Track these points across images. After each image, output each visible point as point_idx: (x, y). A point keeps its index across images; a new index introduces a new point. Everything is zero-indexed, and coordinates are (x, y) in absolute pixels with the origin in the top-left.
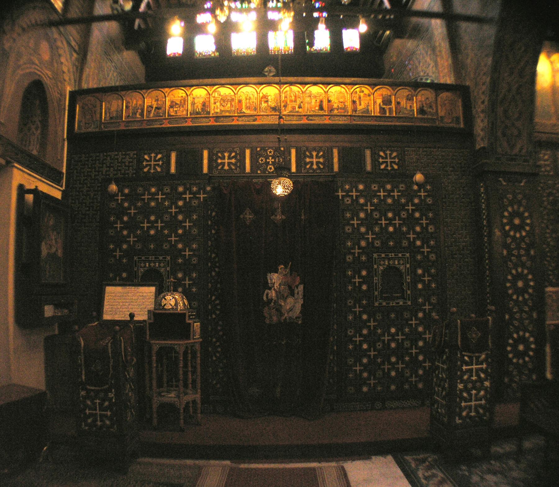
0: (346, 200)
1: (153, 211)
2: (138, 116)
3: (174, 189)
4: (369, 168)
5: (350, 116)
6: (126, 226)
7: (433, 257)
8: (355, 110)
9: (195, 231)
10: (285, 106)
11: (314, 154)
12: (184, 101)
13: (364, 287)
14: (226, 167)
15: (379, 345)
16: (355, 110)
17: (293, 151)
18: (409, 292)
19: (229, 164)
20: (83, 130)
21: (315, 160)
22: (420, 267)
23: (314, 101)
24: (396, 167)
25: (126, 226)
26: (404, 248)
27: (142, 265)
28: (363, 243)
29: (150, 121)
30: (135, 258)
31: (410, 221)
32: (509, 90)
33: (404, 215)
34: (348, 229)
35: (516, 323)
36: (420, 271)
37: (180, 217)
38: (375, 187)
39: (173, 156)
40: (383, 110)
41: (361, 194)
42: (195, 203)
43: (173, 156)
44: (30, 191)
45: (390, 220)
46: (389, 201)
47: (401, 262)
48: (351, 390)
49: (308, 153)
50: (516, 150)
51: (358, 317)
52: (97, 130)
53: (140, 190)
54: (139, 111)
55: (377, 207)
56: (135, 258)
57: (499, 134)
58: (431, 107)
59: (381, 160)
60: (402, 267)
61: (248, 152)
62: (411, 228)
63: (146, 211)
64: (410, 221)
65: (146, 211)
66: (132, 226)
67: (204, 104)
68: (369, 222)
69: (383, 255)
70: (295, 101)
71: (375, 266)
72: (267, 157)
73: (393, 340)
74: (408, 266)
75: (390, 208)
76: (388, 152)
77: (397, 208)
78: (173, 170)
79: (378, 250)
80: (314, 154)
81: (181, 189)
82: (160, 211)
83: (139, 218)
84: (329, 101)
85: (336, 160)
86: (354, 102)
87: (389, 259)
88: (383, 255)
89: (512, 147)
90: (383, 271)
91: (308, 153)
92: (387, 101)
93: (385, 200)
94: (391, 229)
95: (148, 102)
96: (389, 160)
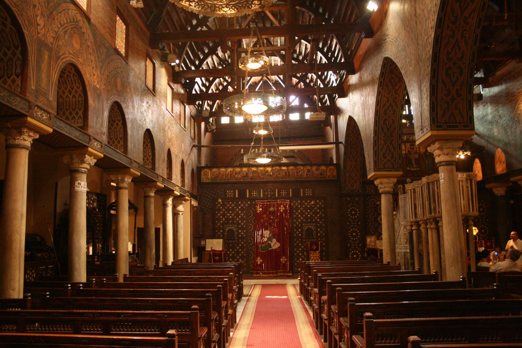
1: (230, 210)
3: (237, 202)
4: (302, 195)
8: (298, 175)
9: (245, 217)
12: (239, 173)
13: (300, 235)
16: (298, 175)
17: (277, 190)
28: (300, 220)
29: (228, 179)
31: (316, 213)
33: (313, 211)
34: (295, 216)
35: (353, 248)
37: (240, 212)
38: (304, 201)
39: (237, 191)
40: (307, 175)
43: (237, 191)
50: (355, 187)
51: (298, 245)
53: (226, 203)
61: (262, 190)
62: (316, 215)
63: (228, 210)
65: (228, 210)
66: (224, 215)
67: (247, 174)
68: (302, 214)
75: (309, 208)
77: (311, 208)
78: (237, 196)
79: (304, 223)
81: (240, 203)
82: (233, 210)
84: (289, 172)
85: (291, 193)
86: (297, 172)
92: (309, 171)
94: (309, 216)
95: (227, 173)
96: (309, 192)
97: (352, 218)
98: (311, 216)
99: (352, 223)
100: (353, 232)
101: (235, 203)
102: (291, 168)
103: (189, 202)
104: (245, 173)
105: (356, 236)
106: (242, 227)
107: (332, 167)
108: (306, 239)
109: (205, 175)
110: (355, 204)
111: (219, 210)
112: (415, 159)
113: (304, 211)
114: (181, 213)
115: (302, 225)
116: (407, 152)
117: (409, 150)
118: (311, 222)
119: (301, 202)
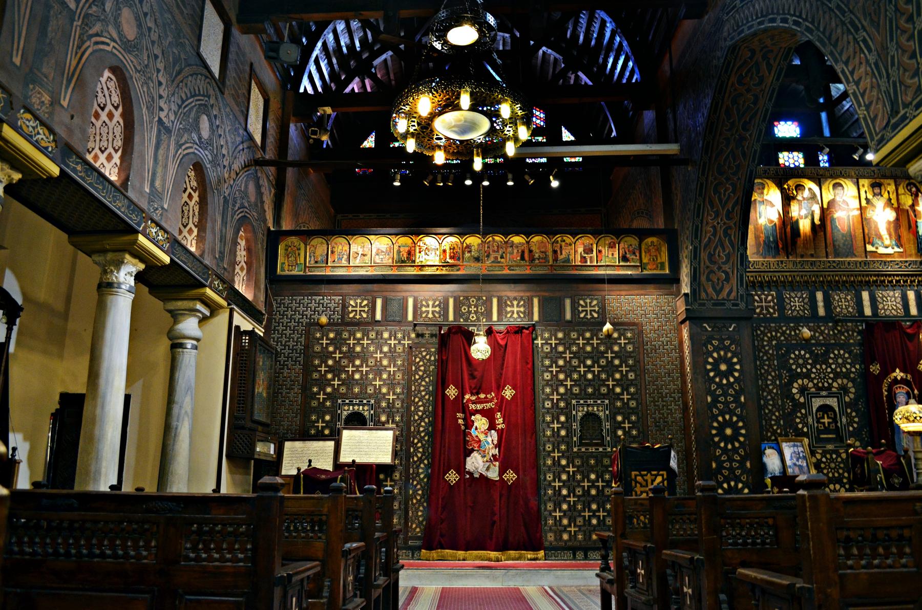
0: (545, 347)
2: (343, 261)
4: (568, 316)
5: (551, 266)
6: (331, 369)
7: (633, 404)
8: (556, 260)
10: (488, 256)
11: (515, 303)
13: (563, 433)
14: (430, 315)
15: (579, 491)
18: (609, 438)
19: (433, 312)
20: (287, 273)
21: (515, 309)
22: (619, 414)
23: (515, 251)
24: (596, 315)
25: (331, 369)
26: (603, 394)
27: (346, 408)
30: (339, 401)
31: (610, 369)
32: (714, 234)
33: (603, 362)
36: (619, 418)
38: (574, 335)
39: (379, 302)
40: (584, 259)
41: (561, 342)
42: (399, 349)
44: (246, 333)
45: (589, 367)
46: (589, 349)
47: (600, 409)
48: (551, 537)
49: (509, 303)
51: (556, 463)
52: (301, 273)
53: (345, 335)
54: (345, 257)
55: (575, 355)
56: (339, 401)
57: (703, 278)
58: (634, 253)
59: (580, 309)
60: (601, 414)
62: (611, 375)
64: (610, 369)
66: (337, 370)
67: (409, 253)
69: (582, 402)
70: (498, 251)
71: (574, 413)
72: (469, 306)
73: (593, 486)
74: (607, 412)
75: (589, 355)
76: (588, 301)
77: (596, 355)
78: (378, 317)
79: (576, 396)
80: (515, 303)
83: (344, 362)
84: (531, 251)
86: (555, 252)
87: (588, 405)
88: (582, 402)
89: (718, 293)
90: (582, 418)
91: (509, 303)
93: (583, 348)
94: (590, 376)
97: (720, 385)
98: (596, 377)
99: (722, 399)
100: (726, 424)
101: (372, 335)
102: (536, 239)
103: (225, 315)
104: (404, 251)
105: (734, 437)
106: (390, 405)
107: (654, 239)
108: (581, 444)
109: (287, 256)
110: (727, 343)
111: (325, 356)
112: (889, 223)
113: (575, 362)
114: (189, 343)
115: (568, 404)
116: (864, 203)
117: (870, 196)
118: (597, 395)
119: (567, 335)
